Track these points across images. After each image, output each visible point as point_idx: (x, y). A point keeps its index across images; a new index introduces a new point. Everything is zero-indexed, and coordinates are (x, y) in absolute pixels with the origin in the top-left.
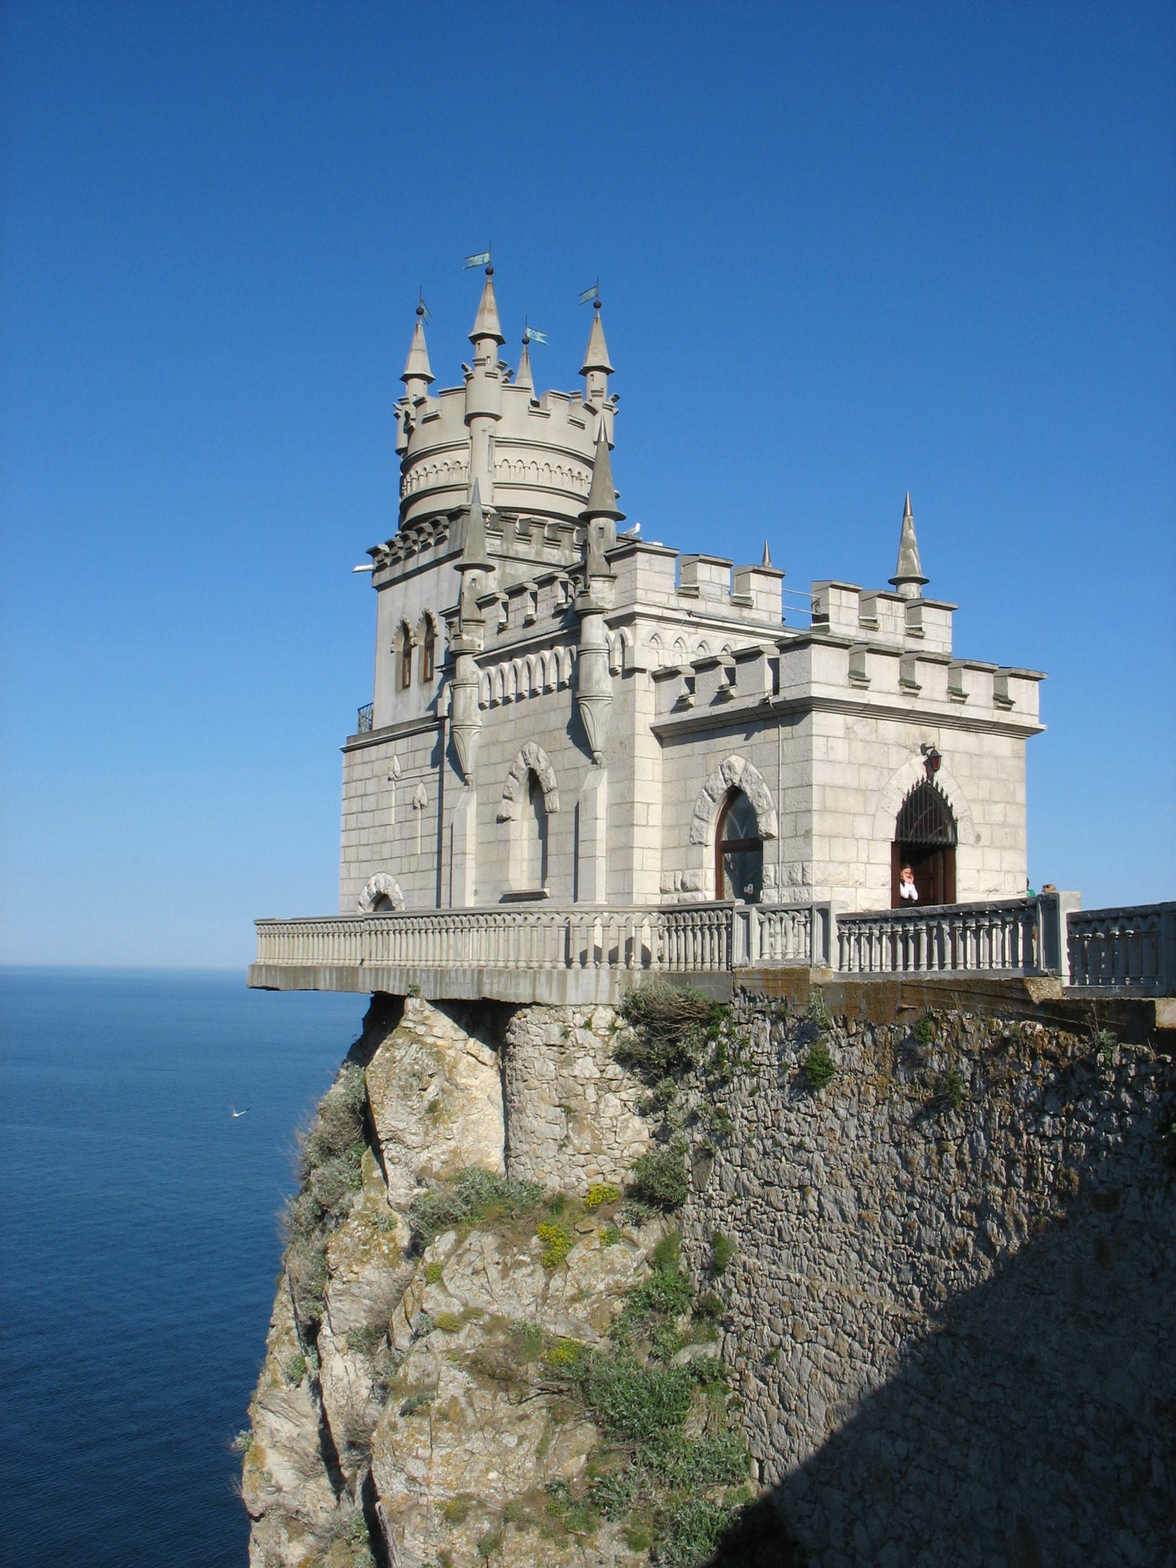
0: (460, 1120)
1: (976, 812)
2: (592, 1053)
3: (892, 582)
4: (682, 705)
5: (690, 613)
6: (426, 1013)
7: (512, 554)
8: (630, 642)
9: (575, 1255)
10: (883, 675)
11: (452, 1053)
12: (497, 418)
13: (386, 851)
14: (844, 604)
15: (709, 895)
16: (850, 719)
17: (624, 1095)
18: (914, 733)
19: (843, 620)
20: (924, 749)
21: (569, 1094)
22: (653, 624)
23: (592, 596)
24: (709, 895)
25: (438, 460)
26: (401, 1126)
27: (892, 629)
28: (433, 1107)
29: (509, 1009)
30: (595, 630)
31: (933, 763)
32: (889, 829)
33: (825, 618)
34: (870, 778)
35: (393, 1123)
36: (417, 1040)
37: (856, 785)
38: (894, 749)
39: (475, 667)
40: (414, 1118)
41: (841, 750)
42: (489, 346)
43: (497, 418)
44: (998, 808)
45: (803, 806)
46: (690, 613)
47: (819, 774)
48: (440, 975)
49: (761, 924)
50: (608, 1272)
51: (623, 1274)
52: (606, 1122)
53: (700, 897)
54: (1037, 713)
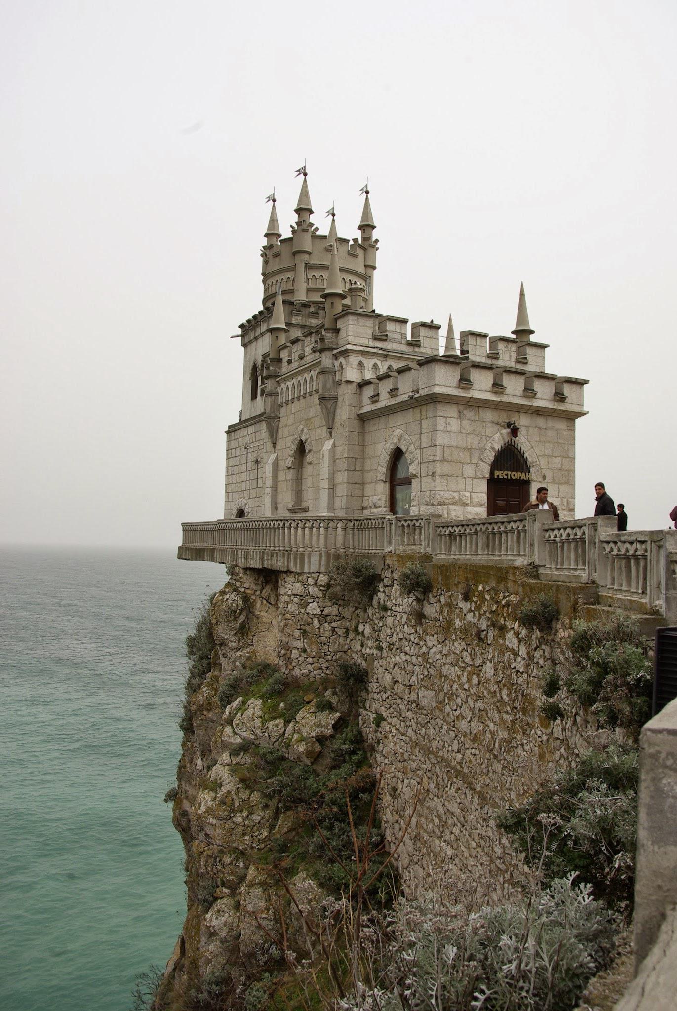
1: (543, 462)
3: (513, 332)
5: (381, 349)
7: (308, 324)
9: (299, 717)
11: (253, 597)
13: (244, 486)
14: (478, 343)
16: (461, 408)
18: (503, 417)
20: (509, 425)
25: (278, 278)
26: (226, 637)
33: (467, 352)
34: (473, 441)
37: (464, 445)
38: (489, 425)
39: (275, 385)
40: (233, 633)
41: (455, 425)
43: (309, 253)
44: (558, 460)
45: (431, 458)
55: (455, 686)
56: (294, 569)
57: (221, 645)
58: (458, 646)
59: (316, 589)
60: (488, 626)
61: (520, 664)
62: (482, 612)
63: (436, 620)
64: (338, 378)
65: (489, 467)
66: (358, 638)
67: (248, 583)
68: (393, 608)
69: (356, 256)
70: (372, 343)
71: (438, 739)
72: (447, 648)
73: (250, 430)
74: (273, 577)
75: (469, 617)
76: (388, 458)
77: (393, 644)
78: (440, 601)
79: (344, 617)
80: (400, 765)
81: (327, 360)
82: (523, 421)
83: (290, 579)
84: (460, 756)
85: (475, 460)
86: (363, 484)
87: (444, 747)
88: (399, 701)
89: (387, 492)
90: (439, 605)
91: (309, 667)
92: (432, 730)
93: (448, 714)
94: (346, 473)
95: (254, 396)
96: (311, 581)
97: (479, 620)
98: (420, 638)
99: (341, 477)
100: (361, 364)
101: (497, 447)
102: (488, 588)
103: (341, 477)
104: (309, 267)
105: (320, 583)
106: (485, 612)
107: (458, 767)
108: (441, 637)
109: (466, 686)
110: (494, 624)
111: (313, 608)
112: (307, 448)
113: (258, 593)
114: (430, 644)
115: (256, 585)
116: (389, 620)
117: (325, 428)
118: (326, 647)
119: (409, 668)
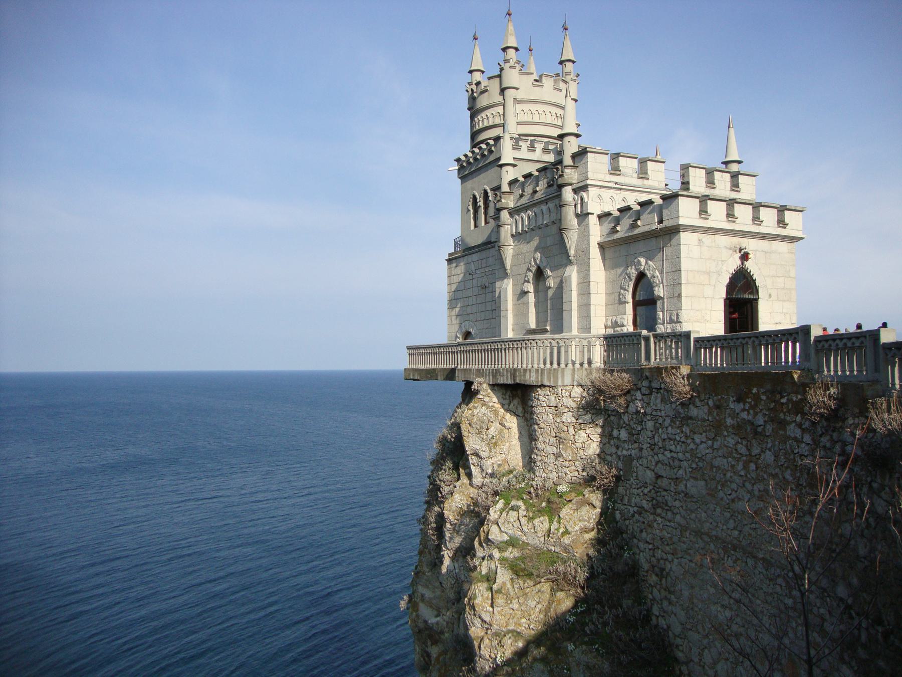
0: (507, 444)
3: (723, 163)
4: (614, 231)
5: (616, 183)
8: (586, 200)
10: (717, 210)
12: (517, 89)
15: (629, 328)
16: (701, 236)
20: (741, 250)
21: (559, 430)
22: (597, 189)
24: (629, 328)
25: (488, 112)
30: (568, 194)
31: (745, 257)
32: (723, 294)
33: (688, 183)
36: (485, 404)
42: (511, 52)
43: (517, 89)
46: (616, 183)
47: (685, 264)
48: (496, 373)
49: (655, 343)
50: (580, 521)
51: (588, 522)
52: (579, 445)
53: (625, 330)
55: (729, 474)
58: (731, 441)
59: (570, 400)
60: (765, 421)
61: (804, 449)
63: (704, 420)
71: (711, 520)
75: (744, 415)
77: (655, 444)
80: (667, 548)
82: (751, 245)
84: (736, 533)
87: (717, 526)
88: (664, 493)
91: (567, 470)
92: (704, 515)
93: (722, 499)
97: (754, 417)
100: (599, 196)
102: (762, 390)
104: (517, 101)
107: (735, 542)
109: (742, 473)
114: (698, 441)
115: (504, 399)
119: (677, 463)
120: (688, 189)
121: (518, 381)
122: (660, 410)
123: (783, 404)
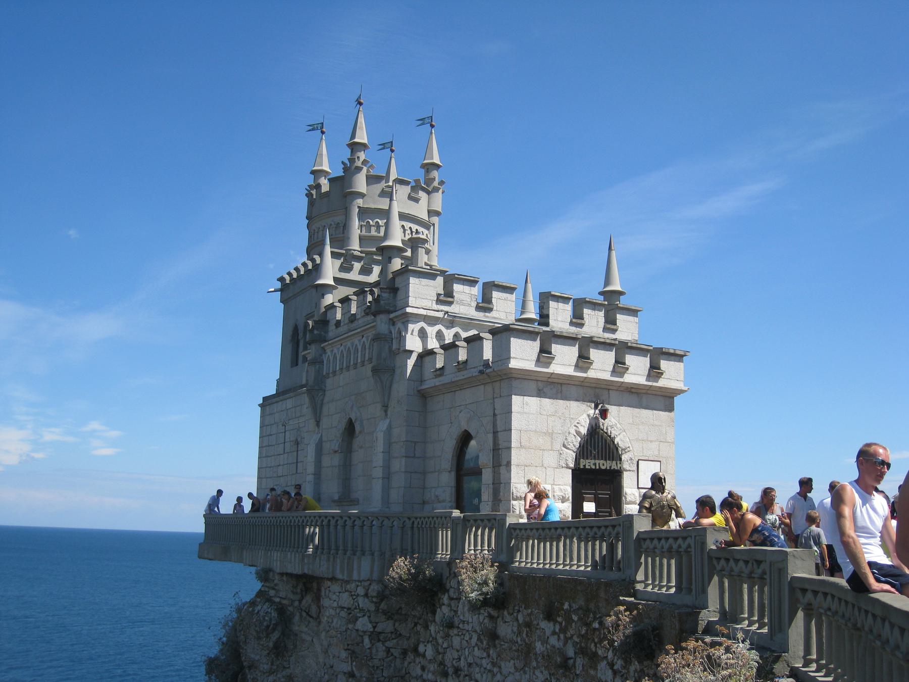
2: (368, 614)
3: (601, 293)
6: (276, 581)
11: (291, 609)
17: (388, 644)
19: (559, 319)
23: (382, 302)
26: (257, 657)
27: (594, 323)
28: (276, 646)
29: (319, 580)
33: (548, 316)
35: (252, 656)
40: (265, 653)
43: (362, 195)
54: (682, 378)
56: (340, 576)
57: (250, 667)
59: (366, 600)
62: (569, 635)
64: (394, 347)
65: (574, 455)
66: (417, 660)
67: (284, 592)
68: (461, 626)
69: (417, 200)
70: (435, 307)
72: (527, 676)
73: (289, 403)
74: (315, 585)
75: (553, 641)
76: (454, 442)
78: (517, 620)
79: (400, 635)
81: (381, 324)
83: (336, 587)
85: (558, 445)
86: (424, 473)
89: (453, 483)
90: (515, 624)
94: (404, 460)
95: (295, 362)
96: (361, 591)
97: (565, 644)
98: (494, 664)
99: (398, 465)
101: (584, 431)
102: (575, 606)
103: (398, 465)
104: (364, 213)
105: (371, 593)
106: (572, 636)
108: (519, 664)
110: (582, 651)
111: (363, 624)
112: (358, 428)
113: (297, 603)
114: (505, 671)
116: (456, 641)
117: (379, 406)
118: (379, 672)
120: (547, 325)
121: (306, 571)
122: (468, 623)
123: (595, 629)
